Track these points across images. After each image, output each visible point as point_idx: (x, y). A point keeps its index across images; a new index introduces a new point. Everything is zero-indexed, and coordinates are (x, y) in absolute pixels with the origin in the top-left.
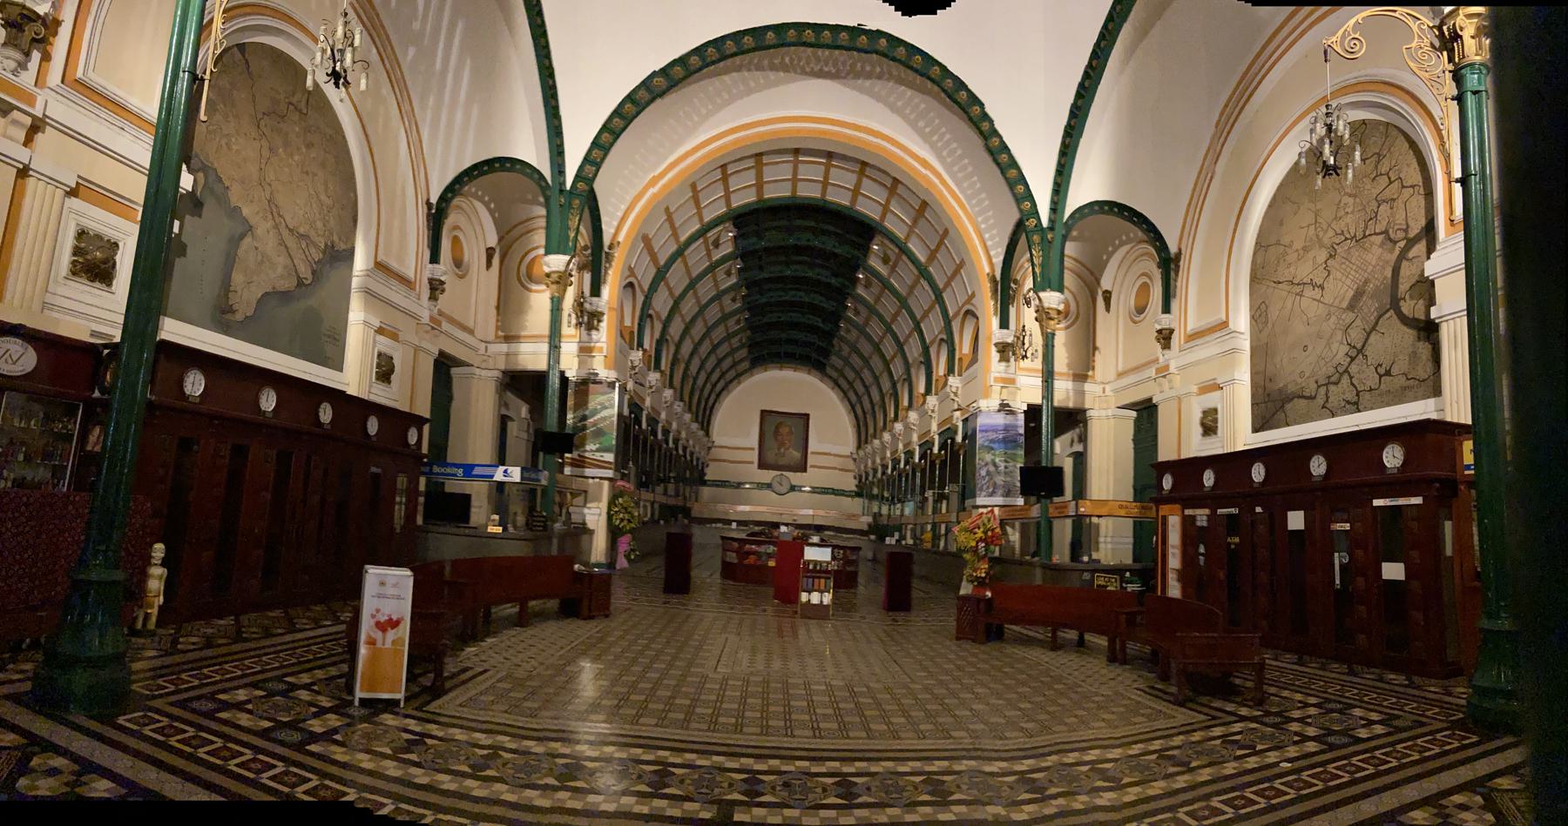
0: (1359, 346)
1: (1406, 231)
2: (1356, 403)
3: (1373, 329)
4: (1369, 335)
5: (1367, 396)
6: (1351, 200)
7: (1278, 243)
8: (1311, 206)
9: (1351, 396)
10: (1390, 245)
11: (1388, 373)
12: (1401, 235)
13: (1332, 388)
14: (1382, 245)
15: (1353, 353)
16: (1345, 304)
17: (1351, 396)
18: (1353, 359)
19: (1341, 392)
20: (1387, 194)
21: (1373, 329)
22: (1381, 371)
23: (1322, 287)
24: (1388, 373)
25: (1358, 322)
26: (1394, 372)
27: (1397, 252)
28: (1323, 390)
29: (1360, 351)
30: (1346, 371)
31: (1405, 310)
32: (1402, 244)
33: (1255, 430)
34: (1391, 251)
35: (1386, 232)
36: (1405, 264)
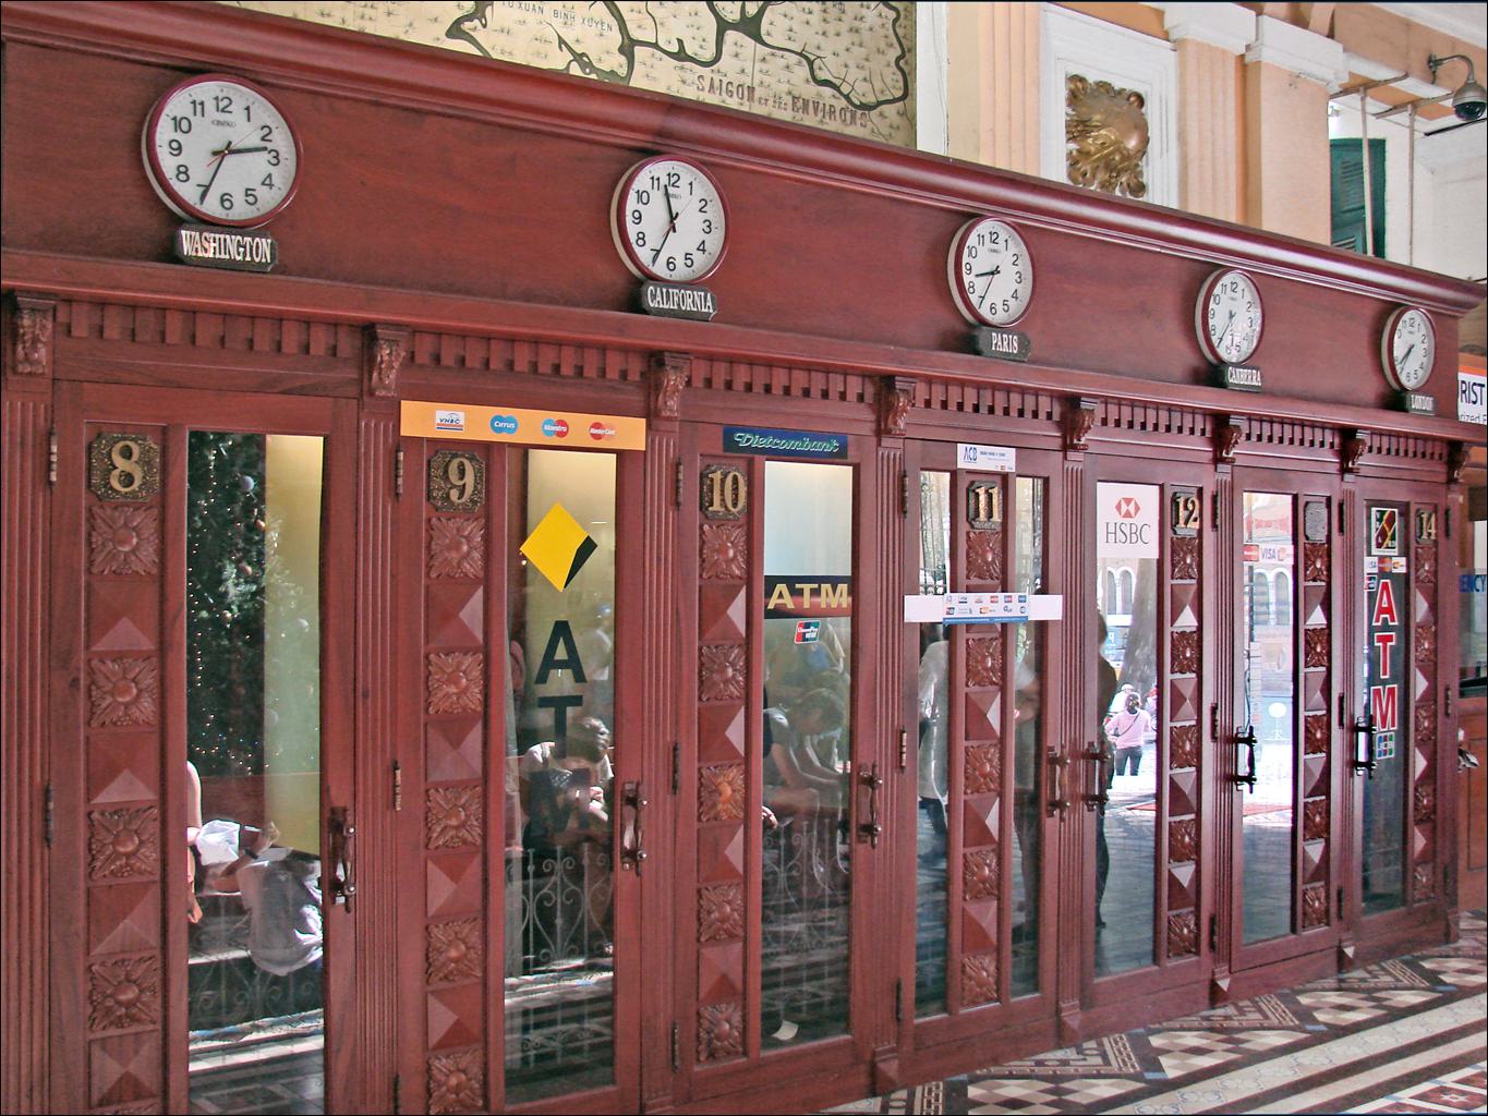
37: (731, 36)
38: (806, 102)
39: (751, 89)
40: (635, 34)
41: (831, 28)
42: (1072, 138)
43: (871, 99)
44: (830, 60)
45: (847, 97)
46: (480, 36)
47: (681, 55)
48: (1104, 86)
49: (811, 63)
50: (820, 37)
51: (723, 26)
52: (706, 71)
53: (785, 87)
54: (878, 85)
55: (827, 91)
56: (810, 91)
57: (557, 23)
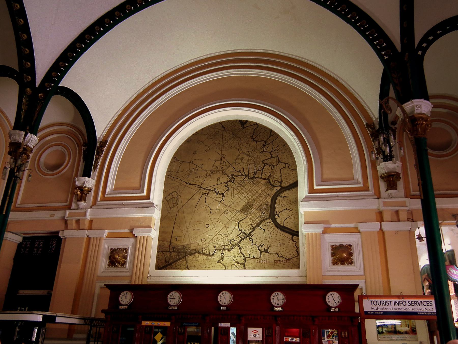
0: (247, 233)
1: (281, 182)
2: (243, 264)
3: (258, 225)
4: (254, 228)
5: (251, 261)
6: (247, 157)
7: (191, 162)
8: (220, 152)
9: (241, 259)
10: (270, 186)
11: (266, 251)
12: (276, 183)
13: (226, 252)
14: (265, 185)
15: (243, 236)
16: (239, 209)
17: (241, 259)
18: (242, 239)
19: (229, 256)
20: (270, 161)
21: (258, 225)
22: (262, 249)
23: (223, 196)
24: (266, 251)
25: (248, 220)
26: (270, 250)
27: (275, 191)
28: (219, 252)
29: (247, 236)
30: (237, 244)
31: (279, 220)
32: (278, 188)
33: (158, 268)
34: (271, 190)
35: (268, 179)
36: (279, 198)
37: (263, 253)
38: (277, 261)
39: (266, 261)
40: (246, 256)
41: (282, 248)
42: (332, 256)
43: (291, 257)
44: (282, 253)
45: (286, 258)
46: (222, 262)
47: (254, 258)
48: (341, 246)
49: (278, 254)
50: (280, 250)
51: (261, 252)
52: (258, 260)
53: (272, 260)
54: (292, 255)
55: (281, 258)
56: (278, 259)
57: (233, 258)
